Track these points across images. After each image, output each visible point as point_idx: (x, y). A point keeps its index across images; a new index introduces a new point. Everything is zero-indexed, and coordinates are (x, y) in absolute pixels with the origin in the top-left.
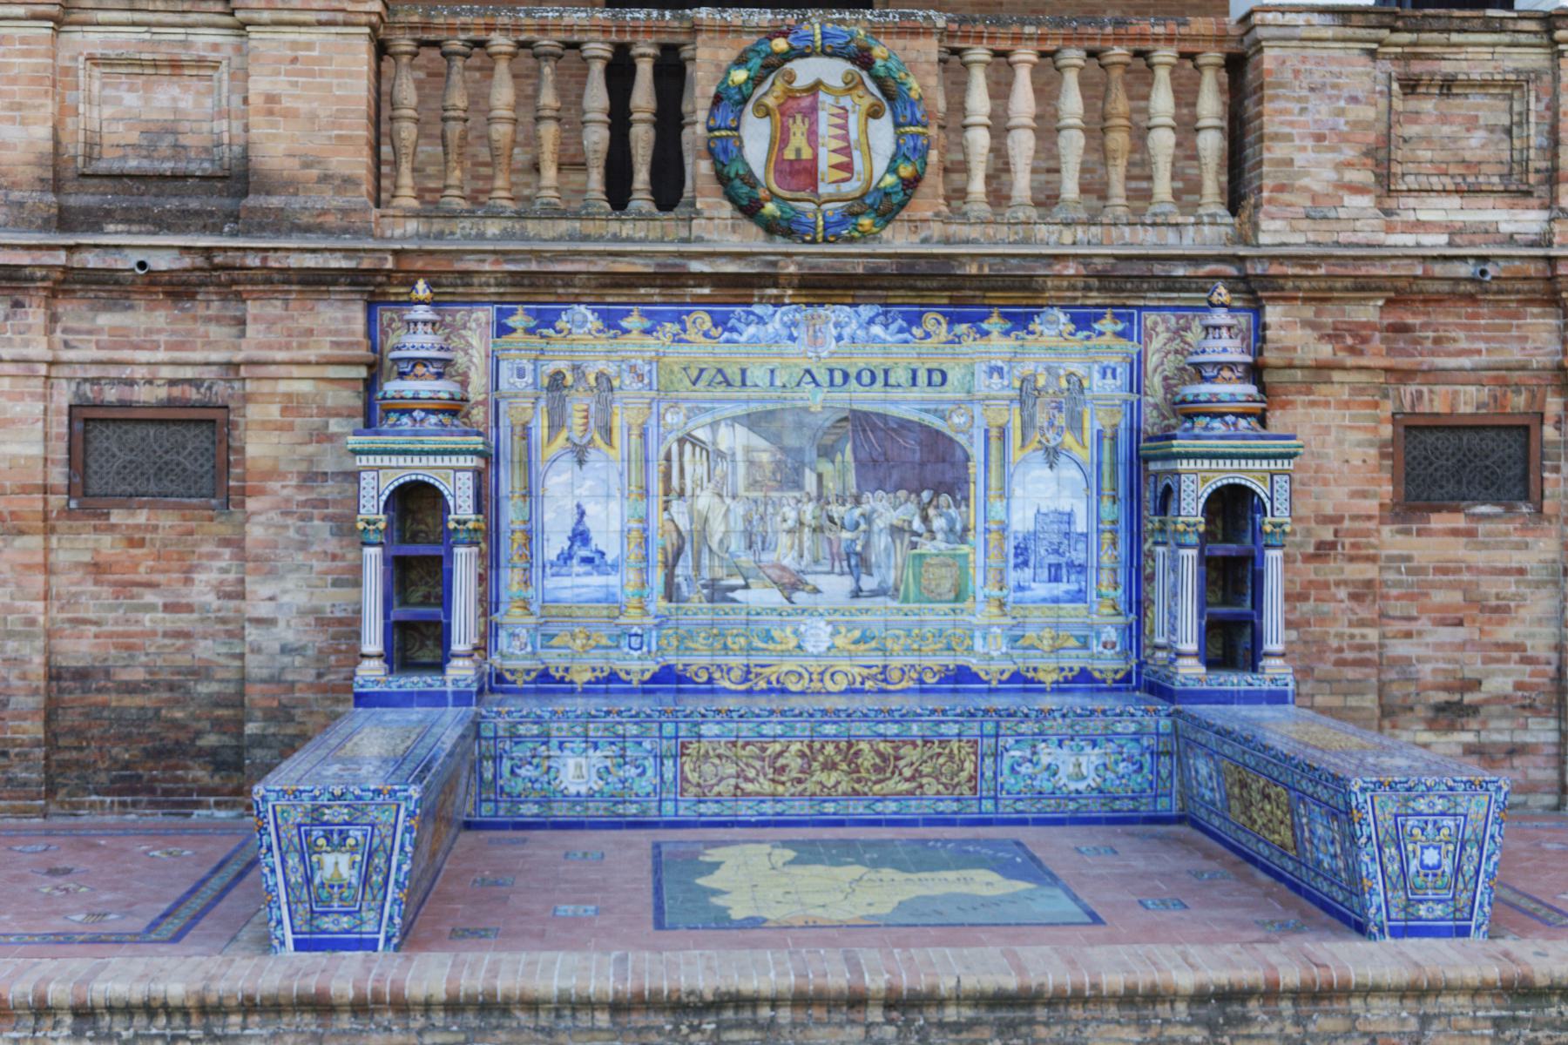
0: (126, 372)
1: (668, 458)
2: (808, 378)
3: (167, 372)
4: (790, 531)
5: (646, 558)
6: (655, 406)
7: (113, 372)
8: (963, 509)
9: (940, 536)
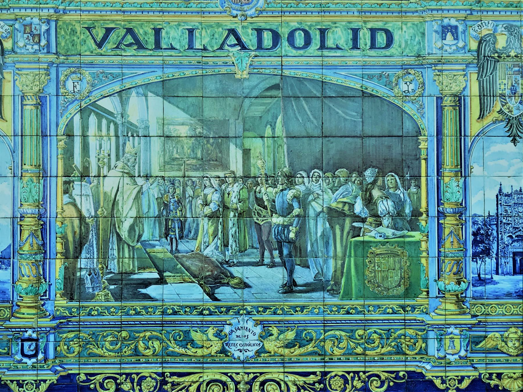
1: (70, 135)
2: (232, 40)
4: (212, 216)
5: (43, 248)
6: (53, 71)
8: (413, 189)
9: (386, 221)
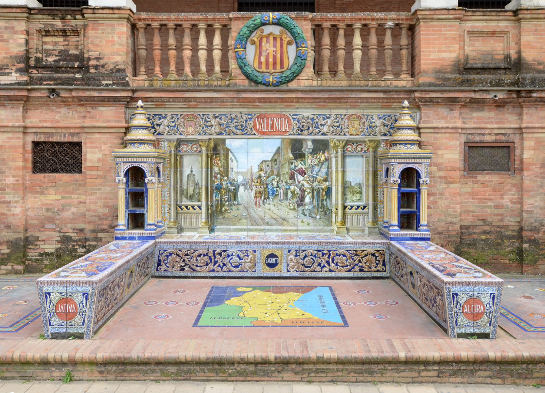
0: (483, 131)
3: (496, 131)
7: (479, 131)
